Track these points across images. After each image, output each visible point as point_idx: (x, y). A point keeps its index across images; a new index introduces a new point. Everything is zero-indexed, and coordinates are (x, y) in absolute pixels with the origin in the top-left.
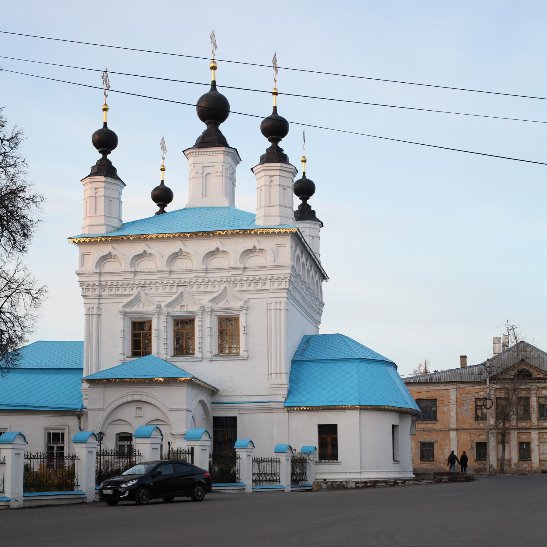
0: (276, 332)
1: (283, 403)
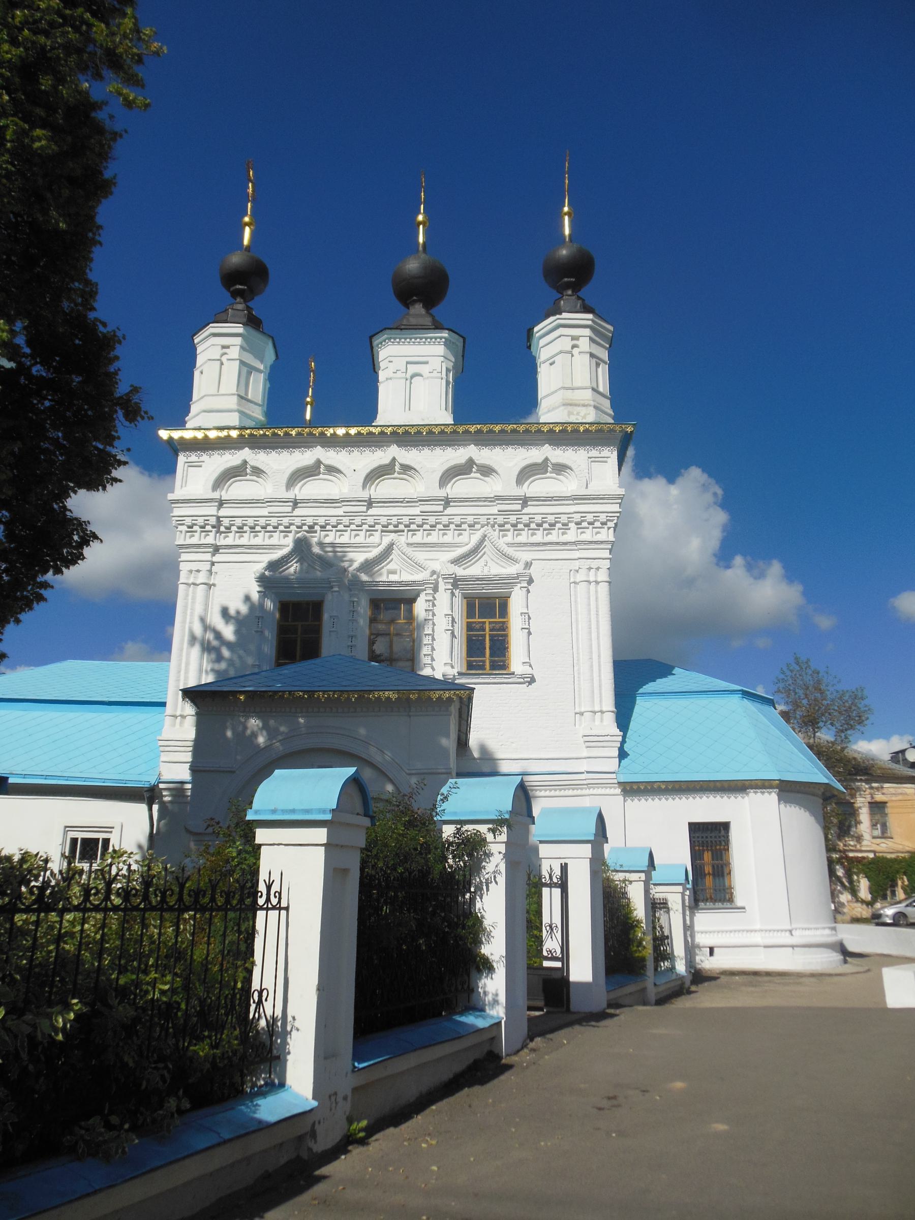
1: (614, 776)
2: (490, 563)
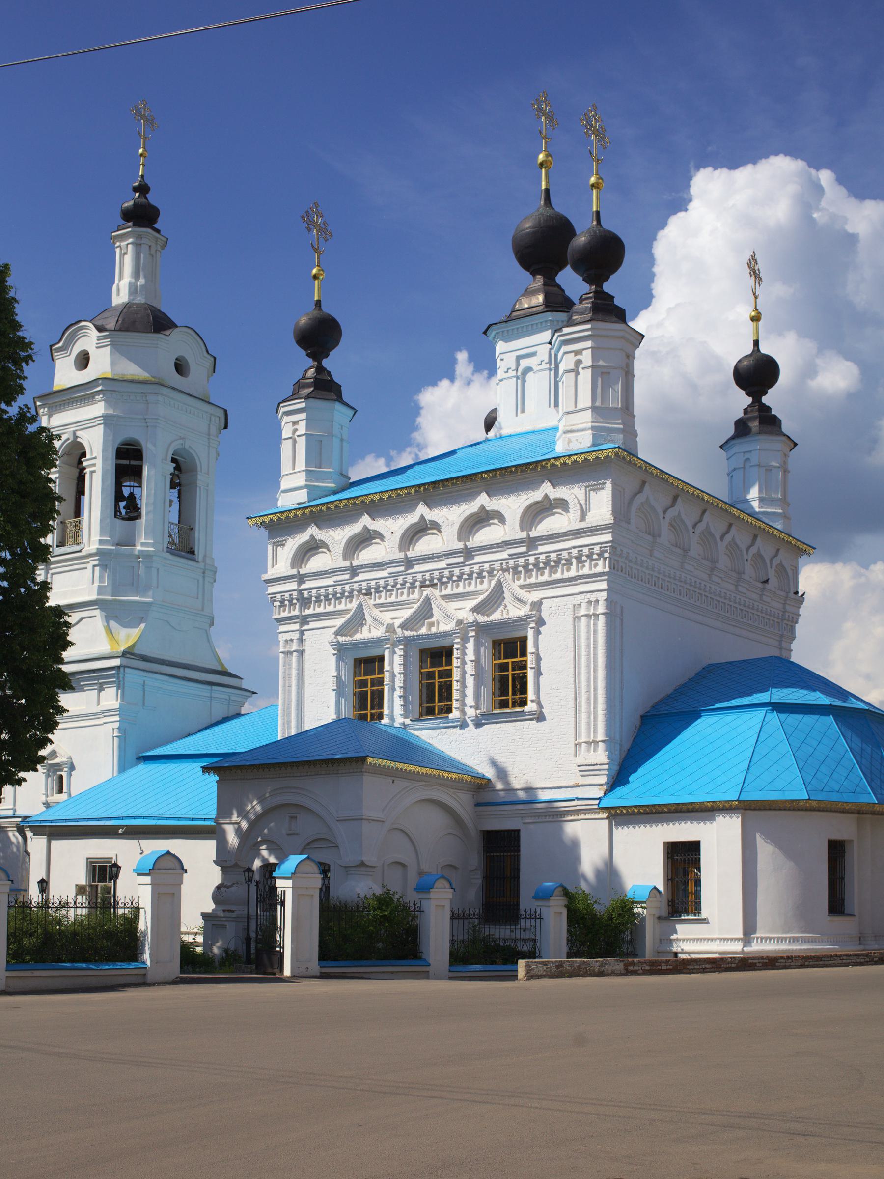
0: (588, 661)
2: (509, 607)
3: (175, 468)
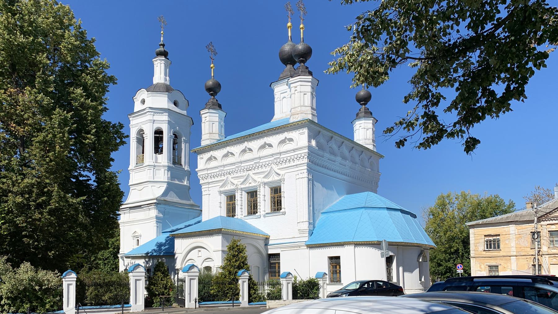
1: (305, 243)
3: (174, 137)
